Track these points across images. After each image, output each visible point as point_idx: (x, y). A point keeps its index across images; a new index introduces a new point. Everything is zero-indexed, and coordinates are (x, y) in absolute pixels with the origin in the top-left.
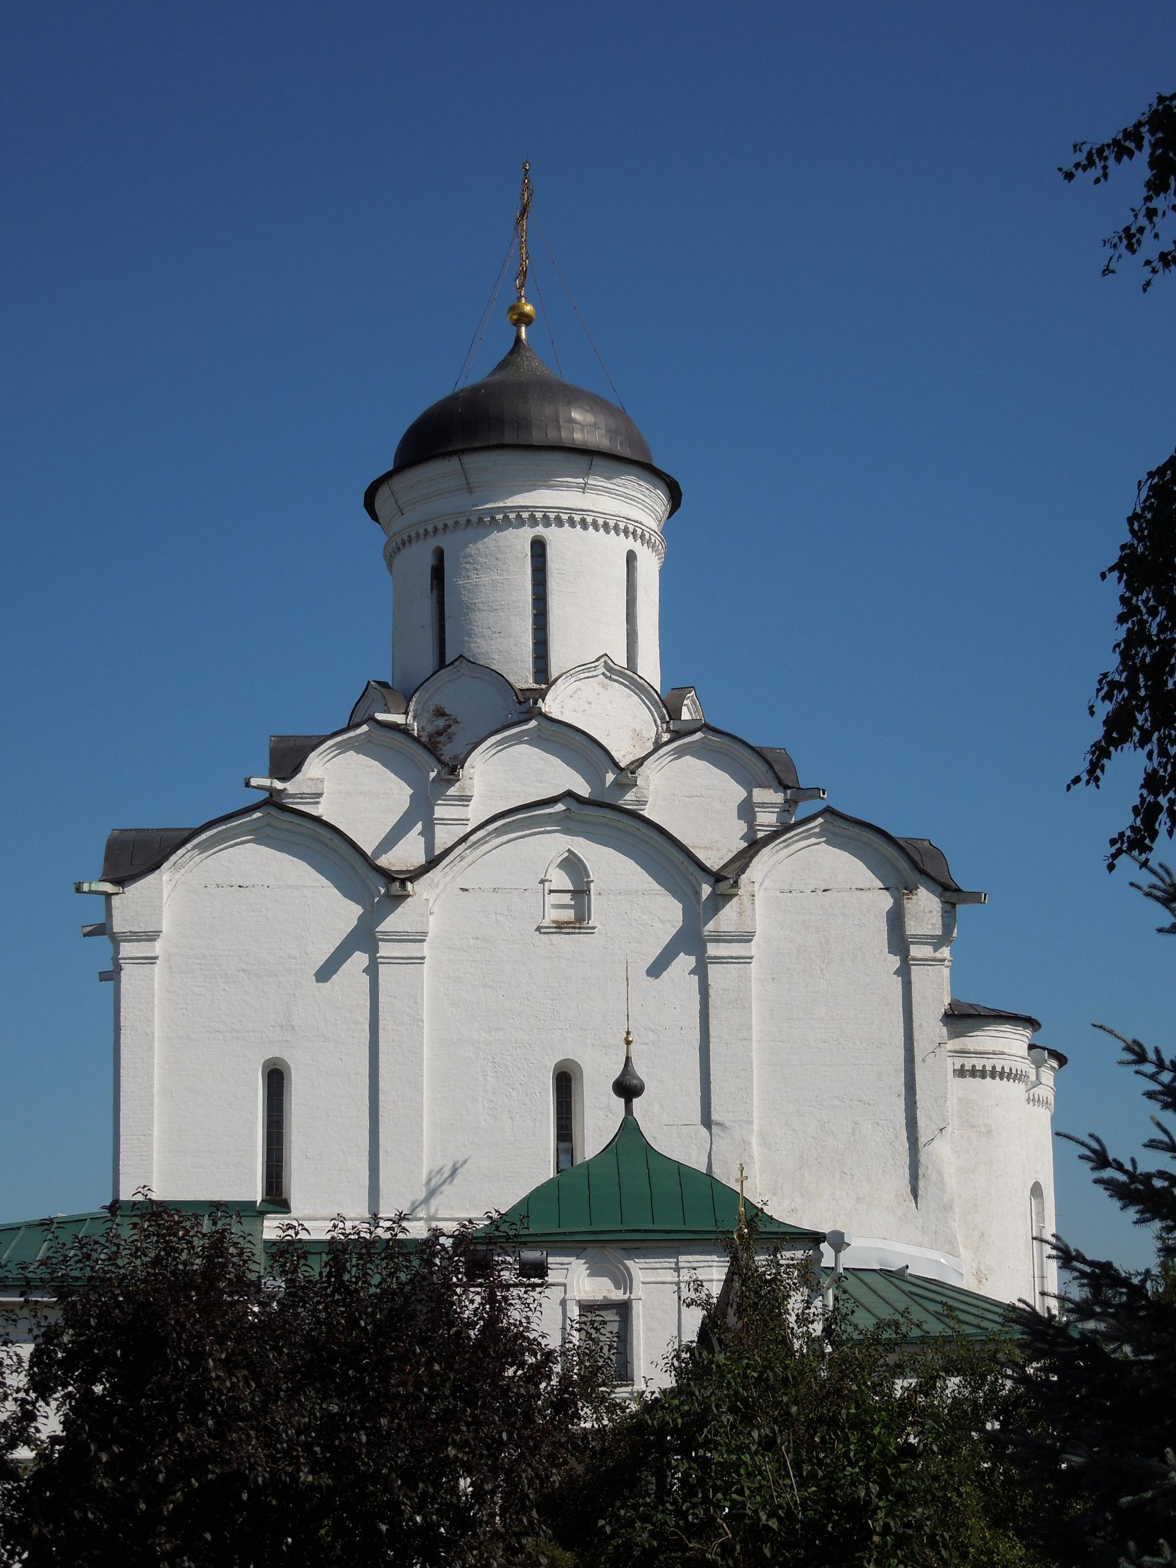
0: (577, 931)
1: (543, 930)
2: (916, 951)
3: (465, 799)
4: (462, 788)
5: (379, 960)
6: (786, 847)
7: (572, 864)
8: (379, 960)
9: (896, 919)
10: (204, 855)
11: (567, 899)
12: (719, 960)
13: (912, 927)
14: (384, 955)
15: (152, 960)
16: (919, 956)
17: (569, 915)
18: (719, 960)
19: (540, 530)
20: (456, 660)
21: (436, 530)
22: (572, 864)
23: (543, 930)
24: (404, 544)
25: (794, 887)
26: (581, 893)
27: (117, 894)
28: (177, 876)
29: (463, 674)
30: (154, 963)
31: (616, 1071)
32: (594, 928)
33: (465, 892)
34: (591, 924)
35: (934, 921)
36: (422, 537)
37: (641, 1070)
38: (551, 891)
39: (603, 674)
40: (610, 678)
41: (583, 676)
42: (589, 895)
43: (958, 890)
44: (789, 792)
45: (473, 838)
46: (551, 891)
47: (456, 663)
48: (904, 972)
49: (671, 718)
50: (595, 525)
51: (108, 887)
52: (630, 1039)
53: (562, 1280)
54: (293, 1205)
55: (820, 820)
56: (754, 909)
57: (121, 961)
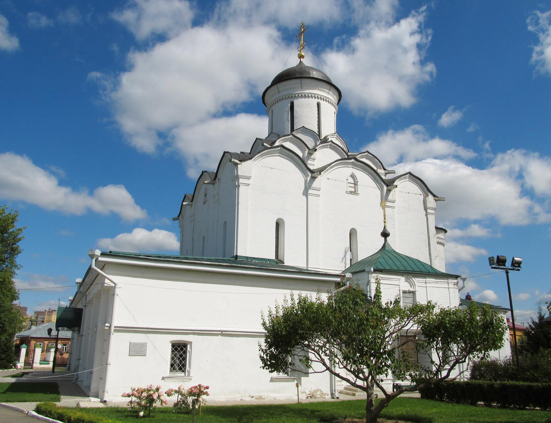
0: (355, 194)
1: (347, 193)
2: (429, 211)
3: (314, 159)
4: (314, 156)
5: (309, 194)
6: (400, 180)
7: (353, 176)
8: (309, 194)
9: (425, 202)
10: (261, 159)
11: (353, 185)
12: (388, 207)
13: (429, 205)
14: (310, 193)
15: (248, 185)
16: (430, 212)
17: (353, 190)
18: (388, 207)
19: (319, 100)
20: (302, 127)
21: (292, 96)
22: (353, 176)
23: (347, 193)
24: (274, 104)
25: (402, 191)
26: (356, 184)
27: (240, 164)
28: (255, 162)
29: (303, 131)
30: (249, 186)
31: (382, 230)
32: (359, 194)
33: (328, 180)
34: (358, 193)
35: (432, 204)
36: (279, 101)
37: (389, 229)
38: (349, 183)
39: (336, 137)
40: (337, 139)
41: (332, 137)
42: (357, 185)
43: (437, 197)
44: (386, 171)
45: (332, 165)
46: (349, 183)
47: (302, 128)
48: (426, 215)
49: (348, 152)
50: (330, 102)
51: (237, 161)
52: (385, 221)
53: (398, 284)
54: (285, 263)
55: (408, 175)
56: (395, 195)
57: (240, 184)
